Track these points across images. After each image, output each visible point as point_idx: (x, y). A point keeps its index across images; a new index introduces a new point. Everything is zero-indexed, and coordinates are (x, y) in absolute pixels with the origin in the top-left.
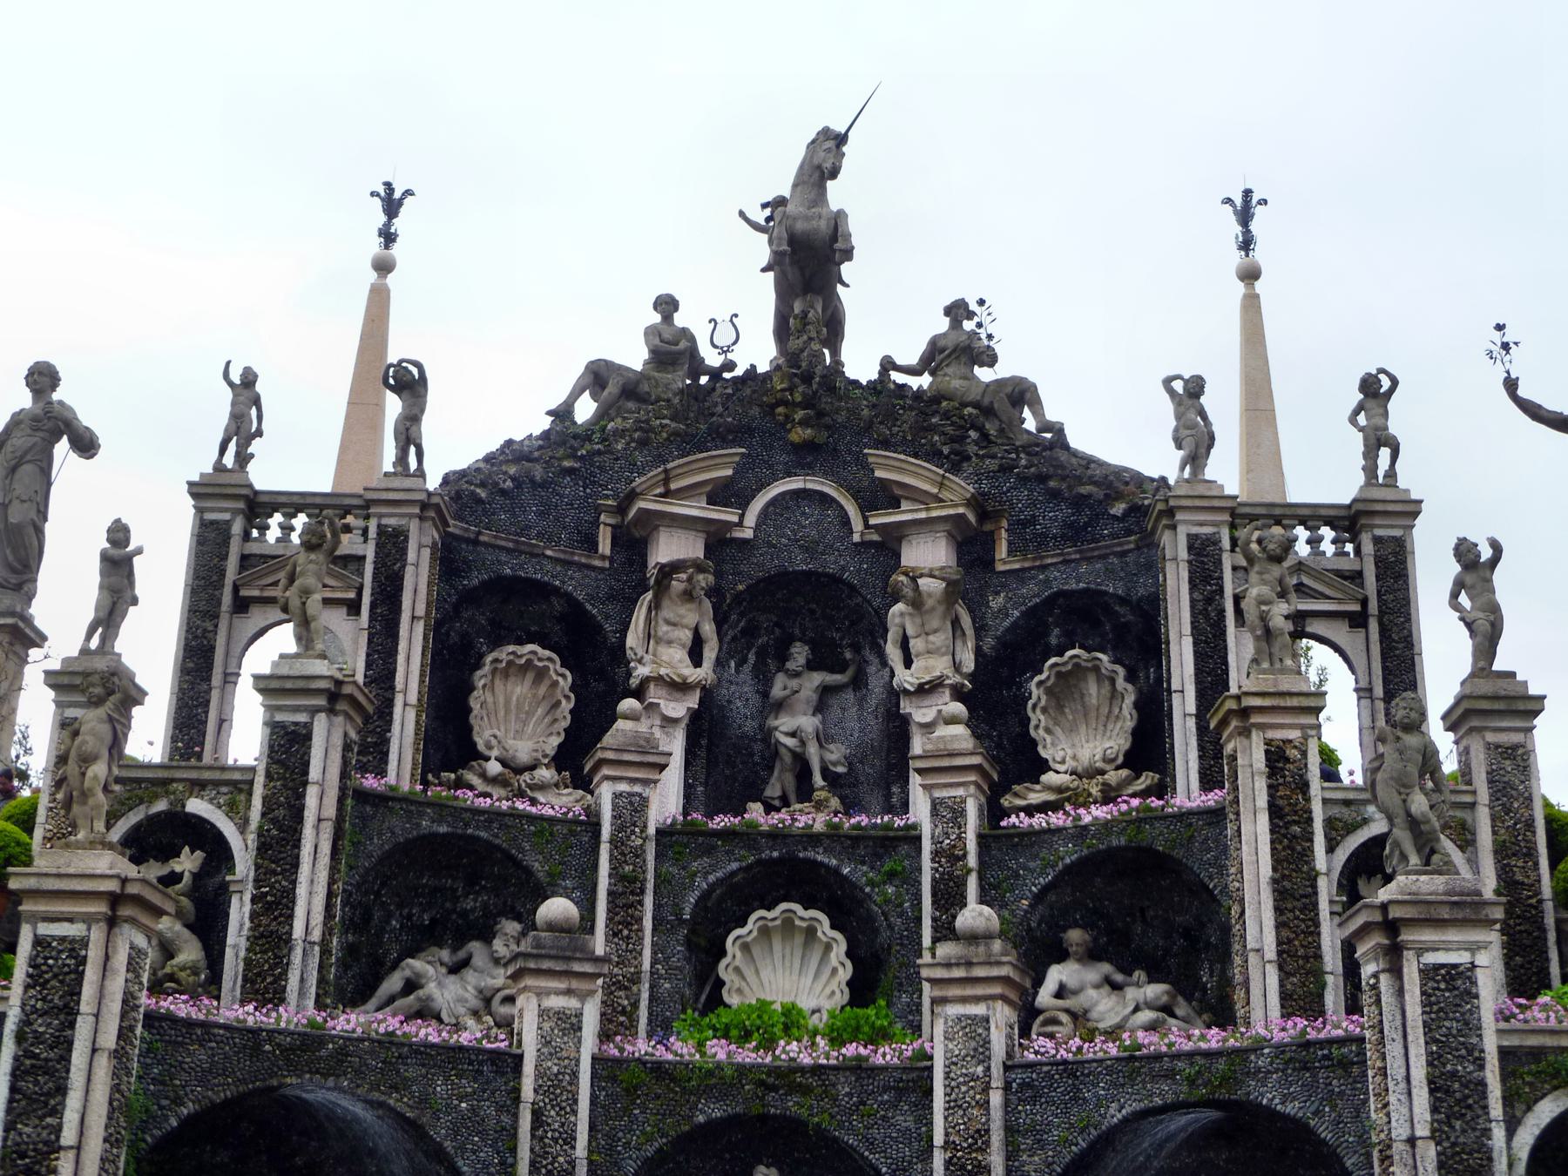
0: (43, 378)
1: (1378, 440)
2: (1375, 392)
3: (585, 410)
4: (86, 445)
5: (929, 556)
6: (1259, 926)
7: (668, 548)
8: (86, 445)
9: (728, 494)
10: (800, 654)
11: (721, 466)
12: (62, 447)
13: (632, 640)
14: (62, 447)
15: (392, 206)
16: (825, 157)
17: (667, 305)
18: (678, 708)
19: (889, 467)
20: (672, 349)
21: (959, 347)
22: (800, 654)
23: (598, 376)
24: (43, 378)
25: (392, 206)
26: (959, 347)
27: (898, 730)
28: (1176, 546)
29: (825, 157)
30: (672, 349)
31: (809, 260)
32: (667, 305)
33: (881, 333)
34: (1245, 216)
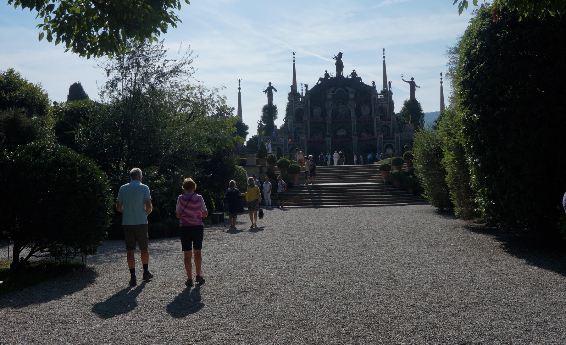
0: (270, 84)
1: (390, 87)
2: (390, 83)
3: (320, 82)
4: (276, 90)
5: (352, 96)
6: (375, 132)
7: (329, 96)
8: (276, 90)
9: (333, 92)
10: (340, 104)
11: (333, 89)
12: (273, 90)
13: (326, 105)
14: (273, 90)
15: (294, 54)
16: (340, 55)
17: (326, 71)
18: (331, 111)
19: (348, 88)
20: (327, 75)
21: (354, 74)
22: (340, 104)
23: (321, 79)
24: (270, 84)
25: (294, 54)
26: (354, 74)
27: (350, 112)
28: (372, 98)
29: (340, 55)
30: (327, 75)
31: (339, 66)
32: (326, 71)
33: (347, 73)
34: (384, 51)
